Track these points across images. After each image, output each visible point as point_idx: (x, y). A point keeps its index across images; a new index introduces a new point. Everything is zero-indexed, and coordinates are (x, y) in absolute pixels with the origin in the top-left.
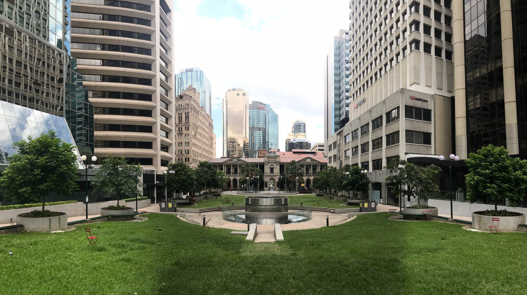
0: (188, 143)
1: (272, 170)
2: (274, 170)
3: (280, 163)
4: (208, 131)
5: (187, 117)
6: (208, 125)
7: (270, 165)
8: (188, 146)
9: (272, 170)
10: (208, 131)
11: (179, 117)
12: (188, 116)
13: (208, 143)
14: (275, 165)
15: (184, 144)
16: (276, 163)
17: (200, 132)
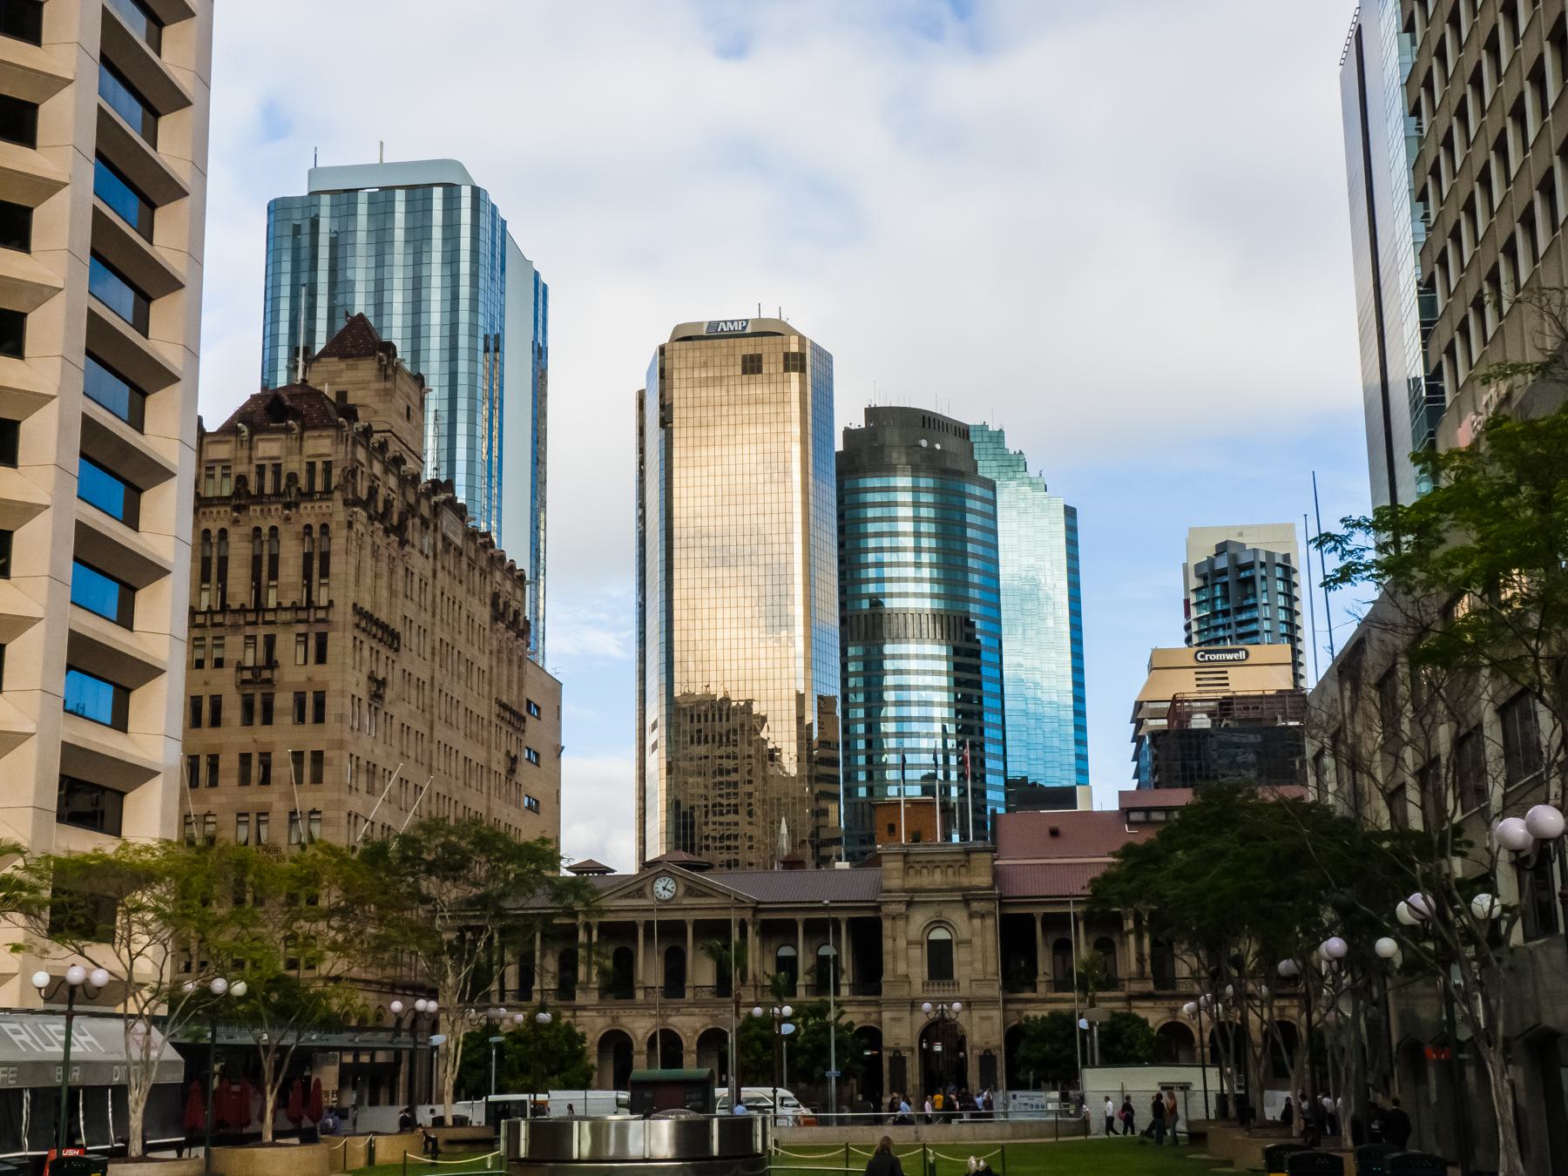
0: (318, 757)
1: (940, 960)
2: (959, 955)
3: (1003, 901)
4: (483, 662)
5: (316, 565)
6: (483, 614)
7: (919, 919)
8: (317, 779)
9: (940, 960)
10: (483, 662)
11: (256, 561)
12: (325, 558)
13: (478, 755)
14: (958, 917)
15: (283, 769)
16: (966, 902)
17: (421, 671)
